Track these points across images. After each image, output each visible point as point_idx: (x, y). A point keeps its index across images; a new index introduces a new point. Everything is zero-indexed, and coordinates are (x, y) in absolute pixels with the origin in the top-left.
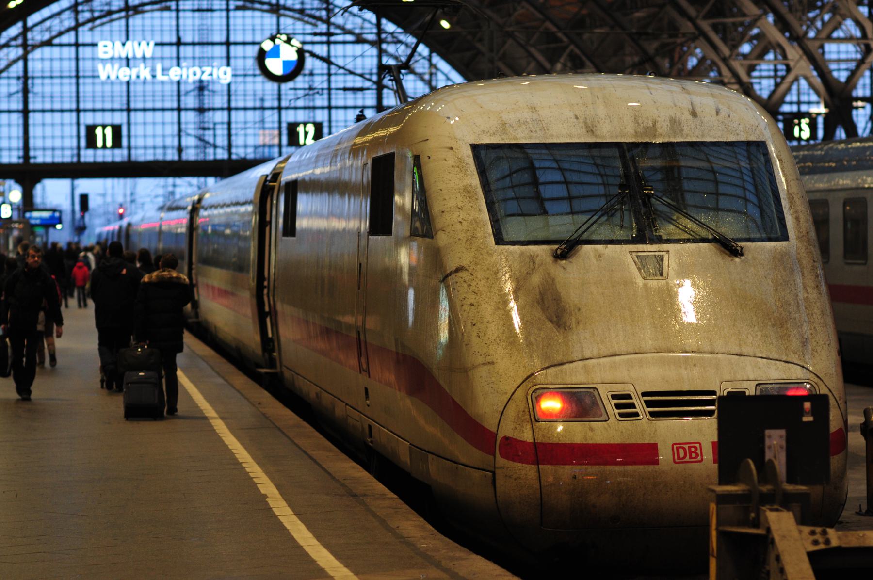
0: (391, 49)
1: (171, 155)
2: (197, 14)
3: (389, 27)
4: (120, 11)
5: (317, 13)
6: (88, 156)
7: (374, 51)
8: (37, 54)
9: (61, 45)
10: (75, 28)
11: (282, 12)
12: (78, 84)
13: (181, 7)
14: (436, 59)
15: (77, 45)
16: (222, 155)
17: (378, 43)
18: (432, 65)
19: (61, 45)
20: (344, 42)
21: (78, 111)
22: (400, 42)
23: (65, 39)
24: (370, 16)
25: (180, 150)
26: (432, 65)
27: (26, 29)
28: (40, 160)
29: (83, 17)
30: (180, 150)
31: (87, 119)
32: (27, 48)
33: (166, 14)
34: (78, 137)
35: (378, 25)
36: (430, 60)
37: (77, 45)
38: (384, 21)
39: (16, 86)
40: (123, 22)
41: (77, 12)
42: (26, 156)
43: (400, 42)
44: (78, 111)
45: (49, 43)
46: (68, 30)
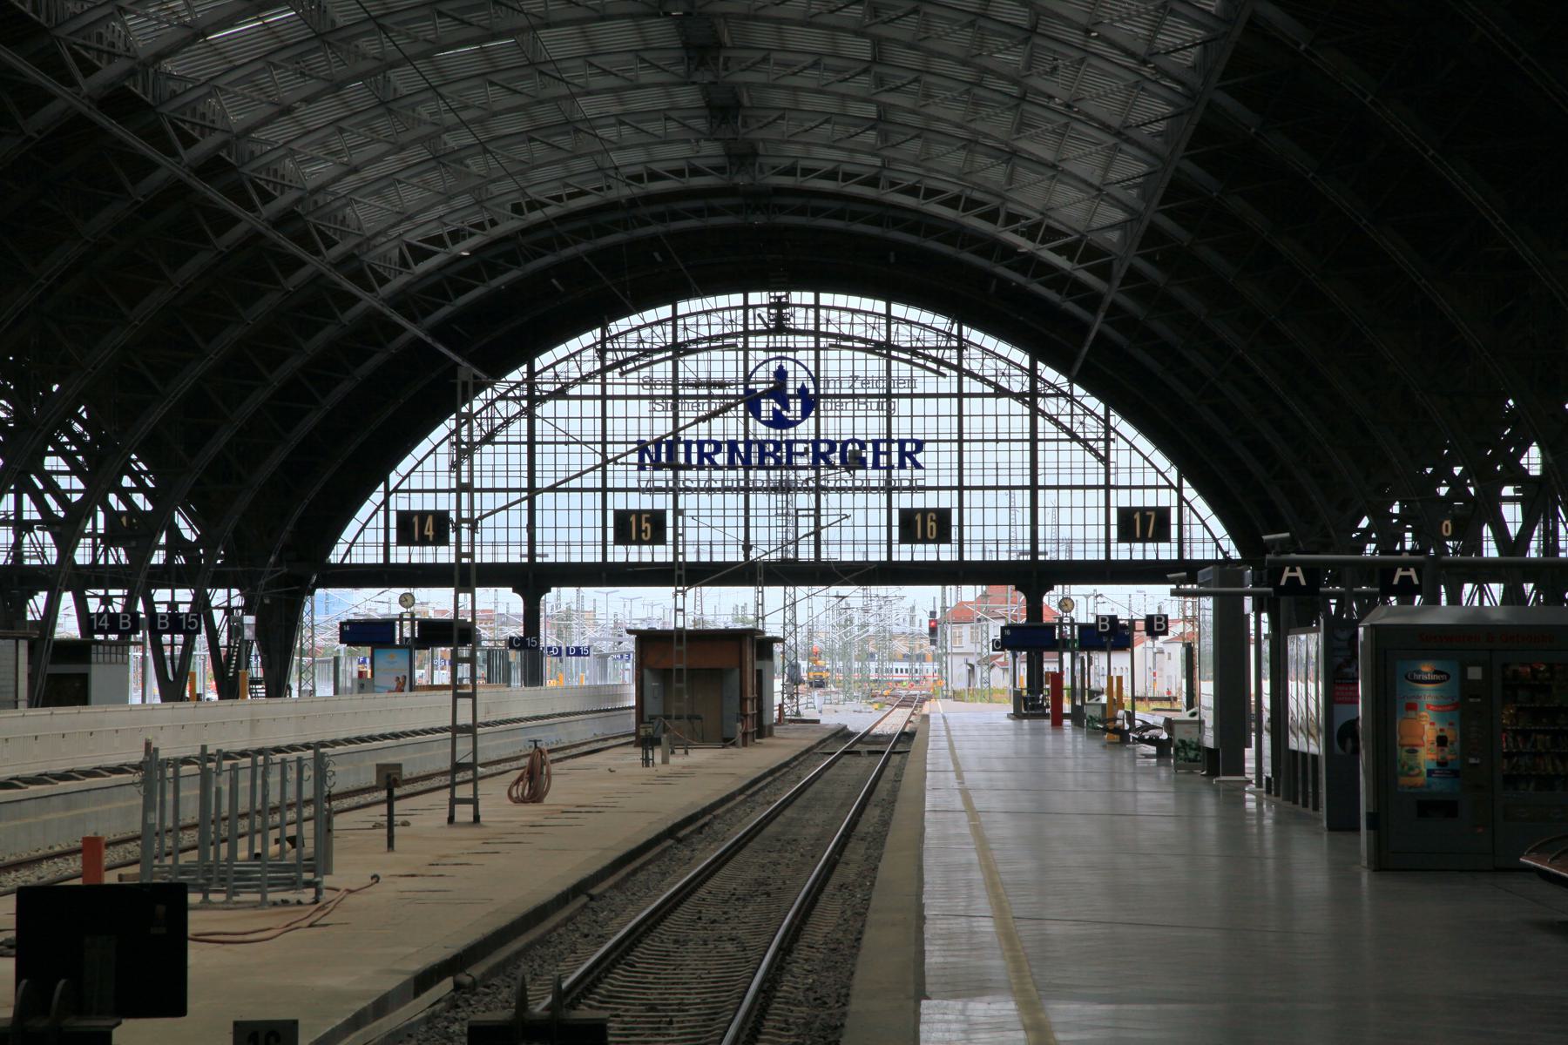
0: (1049, 405)
1: (734, 555)
3: (1048, 373)
7: (1027, 411)
8: (545, 409)
9: (581, 398)
11: (894, 353)
13: (751, 345)
14: (1115, 419)
15: (604, 397)
16: (806, 553)
17: (1030, 398)
18: (1108, 428)
19: (581, 398)
20: (983, 395)
22: (1060, 394)
23: (587, 389)
26: (1108, 428)
27: (532, 373)
28: (550, 559)
30: (747, 547)
32: (534, 400)
33: (730, 355)
35: (1033, 373)
36: (1106, 421)
37: (604, 397)
38: (1040, 365)
39: (519, 457)
40: (669, 363)
41: (602, 353)
42: (532, 554)
43: (1064, 394)
45: (561, 394)
46: (591, 375)
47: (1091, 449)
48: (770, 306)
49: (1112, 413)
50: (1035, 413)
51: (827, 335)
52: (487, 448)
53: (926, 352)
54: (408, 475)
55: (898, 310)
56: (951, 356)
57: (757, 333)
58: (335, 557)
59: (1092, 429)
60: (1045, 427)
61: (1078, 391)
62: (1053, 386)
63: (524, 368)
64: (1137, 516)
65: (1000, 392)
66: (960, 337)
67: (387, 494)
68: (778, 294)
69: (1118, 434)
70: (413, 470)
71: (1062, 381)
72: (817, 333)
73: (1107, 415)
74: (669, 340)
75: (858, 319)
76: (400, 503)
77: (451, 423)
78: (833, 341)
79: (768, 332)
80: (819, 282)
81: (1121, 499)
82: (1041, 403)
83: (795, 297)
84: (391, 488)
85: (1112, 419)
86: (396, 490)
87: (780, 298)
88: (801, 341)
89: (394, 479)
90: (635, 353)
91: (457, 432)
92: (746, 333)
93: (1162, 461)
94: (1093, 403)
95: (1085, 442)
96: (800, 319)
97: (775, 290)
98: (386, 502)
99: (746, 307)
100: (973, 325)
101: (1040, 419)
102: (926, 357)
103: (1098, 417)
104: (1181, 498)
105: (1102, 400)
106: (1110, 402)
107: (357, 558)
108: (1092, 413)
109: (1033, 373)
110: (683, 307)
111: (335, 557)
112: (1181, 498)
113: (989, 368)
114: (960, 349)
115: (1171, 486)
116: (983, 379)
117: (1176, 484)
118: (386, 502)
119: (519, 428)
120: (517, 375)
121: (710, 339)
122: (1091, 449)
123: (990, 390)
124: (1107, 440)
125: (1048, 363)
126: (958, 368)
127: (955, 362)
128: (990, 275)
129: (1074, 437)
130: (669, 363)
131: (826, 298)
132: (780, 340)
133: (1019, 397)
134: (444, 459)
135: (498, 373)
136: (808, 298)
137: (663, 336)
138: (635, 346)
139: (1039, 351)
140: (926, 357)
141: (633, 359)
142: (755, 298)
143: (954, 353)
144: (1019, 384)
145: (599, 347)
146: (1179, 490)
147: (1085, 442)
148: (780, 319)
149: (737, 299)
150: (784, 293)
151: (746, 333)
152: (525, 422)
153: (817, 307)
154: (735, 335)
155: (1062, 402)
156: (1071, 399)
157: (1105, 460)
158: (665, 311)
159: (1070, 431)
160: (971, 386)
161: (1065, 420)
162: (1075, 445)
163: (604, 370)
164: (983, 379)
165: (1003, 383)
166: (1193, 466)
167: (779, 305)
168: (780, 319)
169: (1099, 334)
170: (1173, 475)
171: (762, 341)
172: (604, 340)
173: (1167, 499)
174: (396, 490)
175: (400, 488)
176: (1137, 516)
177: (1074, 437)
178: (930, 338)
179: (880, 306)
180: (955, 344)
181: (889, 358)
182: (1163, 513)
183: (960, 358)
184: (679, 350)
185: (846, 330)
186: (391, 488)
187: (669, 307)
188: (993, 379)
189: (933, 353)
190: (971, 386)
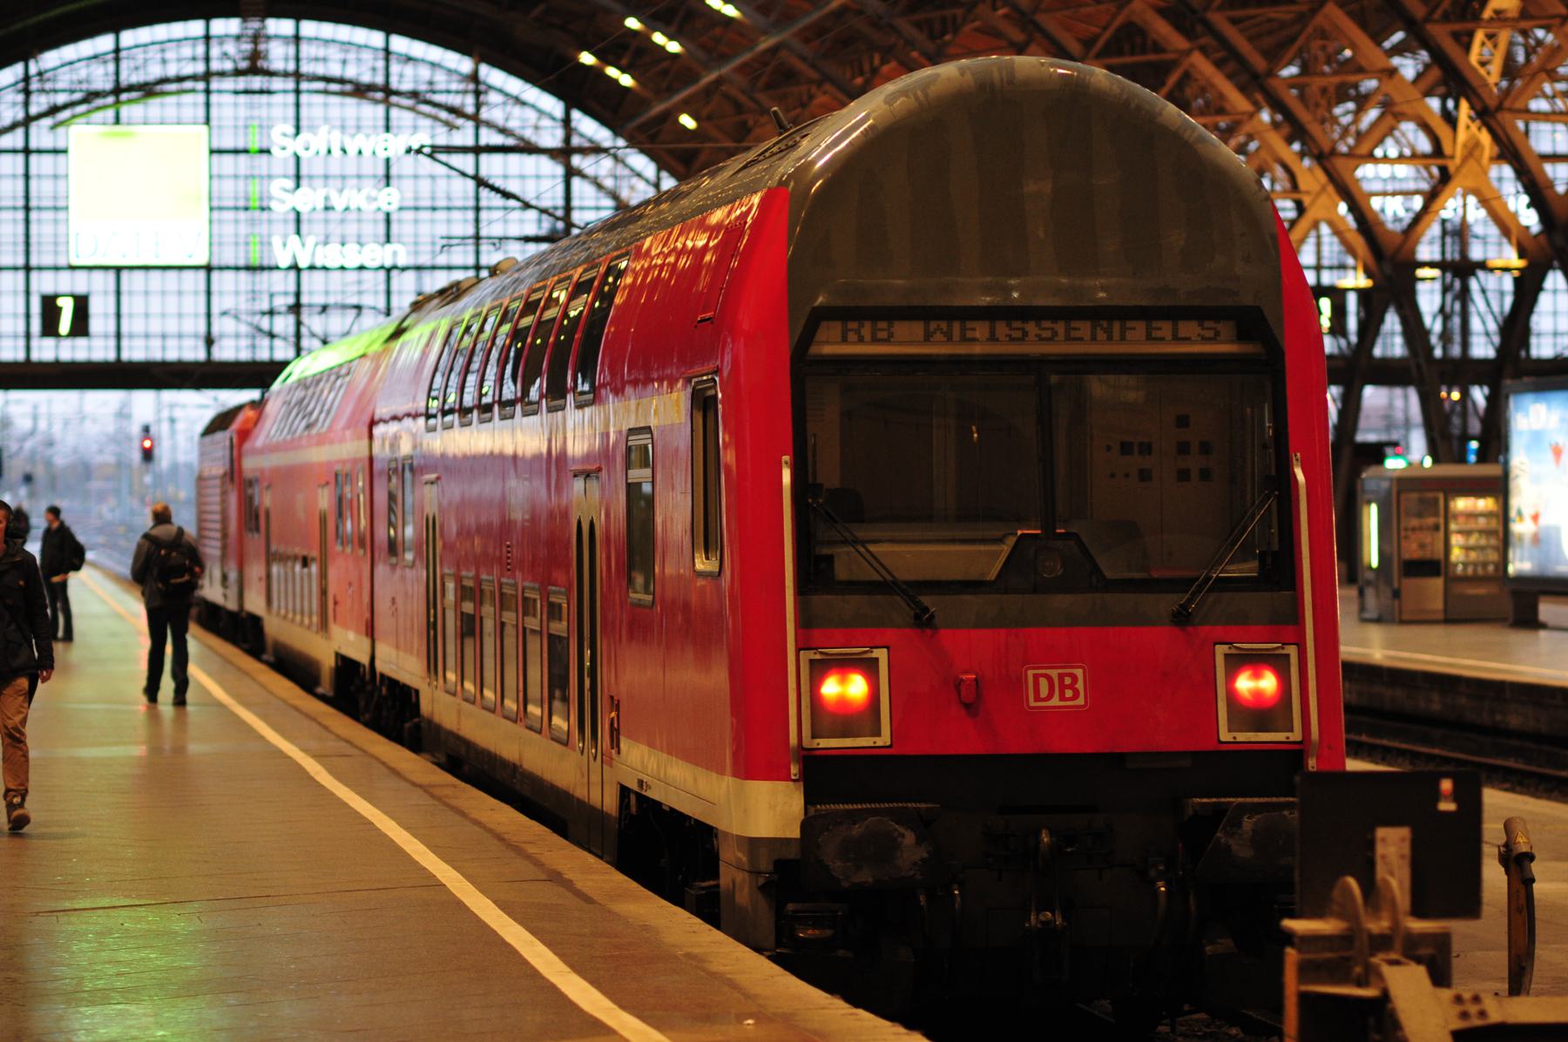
1: (193, 352)
2: (243, 99)
6: (46, 351)
10: (28, 121)
12: (27, 221)
17: (563, 154)
21: (28, 268)
24: (553, 105)
25: (209, 341)
30: (209, 341)
31: (44, 283)
34: (28, 316)
35: (567, 122)
38: (576, 115)
44: (28, 268)
46: (13, 127)
55: (400, 43)
57: (222, 74)
79: (238, 73)
88: (277, 83)
133: (552, 153)
136: (284, 26)
142: (220, 26)
148: (255, 56)
168: (255, 56)
171: (229, 84)
181: (389, 106)
183: (478, 106)
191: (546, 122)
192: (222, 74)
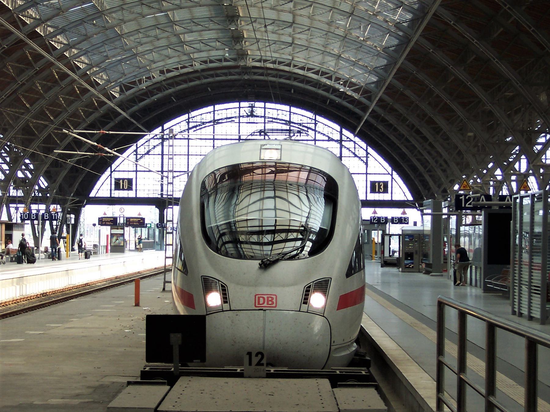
4: (210, 122)
5: (309, 125)
7: (339, 145)
11: (292, 124)
14: (370, 150)
17: (340, 141)
18: (368, 153)
22: (351, 141)
24: (338, 128)
26: (368, 153)
27: (163, 130)
29: (191, 125)
32: (163, 139)
33: (233, 124)
35: (341, 132)
36: (366, 151)
38: (344, 130)
40: (212, 127)
42: (162, 195)
43: (351, 141)
47: (362, 160)
48: (249, 107)
49: (368, 147)
50: (342, 146)
51: (269, 118)
52: (147, 156)
53: (304, 124)
54: (119, 166)
55: (294, 109)
56: (312, 126)
57: (243, 116)
58: (92, 195)
59: (362, 153)
60: (345, 152)
61: (357, 139)
62: (348, 138)
63: (160, 128)
64: (377, 184)
65: (330, 139)
66: (315, 120)
67: (111, 172)
68: (251, 103)
69: (371, 155)
70: (120, 164)
71: (351, 136)
72: (265, 117)
73: (367, 148)
74: (212, 119)
75: (280, 112)
76: (116, 175)
77: (134, 148)
78: (271, 120)
79: (248, 116)
80: (266, 98)
81: (371, 178)
82: (343, 143)
83: (257, 104)
84: (112, 170)
85: (368, 150)
86: (114, 171)
87: (252, 104)
89: (114, 166)
90: (200, 123)
91: (136, 151)
92: (240, 116)
93: (386, 165)
94: (364, 145)
95: (360, 158)
96: (259, 111)
97: (250, 101)
98: (111, 175)
99: (240, 108)
100: (320, 115)
101: (343, 149)
102: (304, 126)
103: (364, 149)
104: (392, 178)
105: (365, 143)
106: (368, 144)
107: (100, 195)
108: (361, 147)
109: (341, 132)
110: (217, 107)
111: (92, 195)
112: (392, 178)
113: (326, 130)
114: (316, 124)
115: (389, 174)
116: (324, 135)
117: (391, 174)
118: (111, 175)
119: (158, 150)
120: (158, 131)
121: (227, 118)
122: (362, 160)
123: (327, 138)
124: (367, 157)
125: (347, 129)
126: (315, 130)
127: (314, 128)
128: (328, 98)
129: (356, 156)
130: (212, 127)
131: (268, 105)
132: (252, 119)
134: (133, 158)
135: (150, 130)
136: (262, 104)
137: (209, 117)
138: (200, 121)
139: (344, 123)
140: (304, 126)
141: (200, 125)
142: (243, 104)
143: (313, 125)
144: (337, 137)
145: (187, 121)
146: (392, 175)
147: (360, 158)
148: (252, 111)
149: (236, 105)
150: (253, 103)
151: (240, 116)
152: (160, 147)
153: (265, 108)
154: (235, 117)
155: (352, 143)
156: (355, 142)
157: (366, 164)
158: (211, 108)
159: (354, 153)
160: (318, 137)
161: (353, 150)
162: (356, 158)
163: (189, 129)
164: (324, 135)
165: (330, 136)
166: (396, 166)
167: (252, 107)
169: (366, 121)
170: (389, 169)
172: (189, 118)
173: (388, 178)
174: (114, 171)
175: (115, 170)
176: (377, 184)
177: (356, 156)
178: (305, 120)
179: (287, 108)
180: (314, 122)
182: (386, 184)
184: (215, 122)
185: (275, 116)
186: (112, 170)
187: (212, 107)
188: (327, 135)
189: (306, 125)
190: (318, 137)
191: (334, 132)
192: (243, 116)
